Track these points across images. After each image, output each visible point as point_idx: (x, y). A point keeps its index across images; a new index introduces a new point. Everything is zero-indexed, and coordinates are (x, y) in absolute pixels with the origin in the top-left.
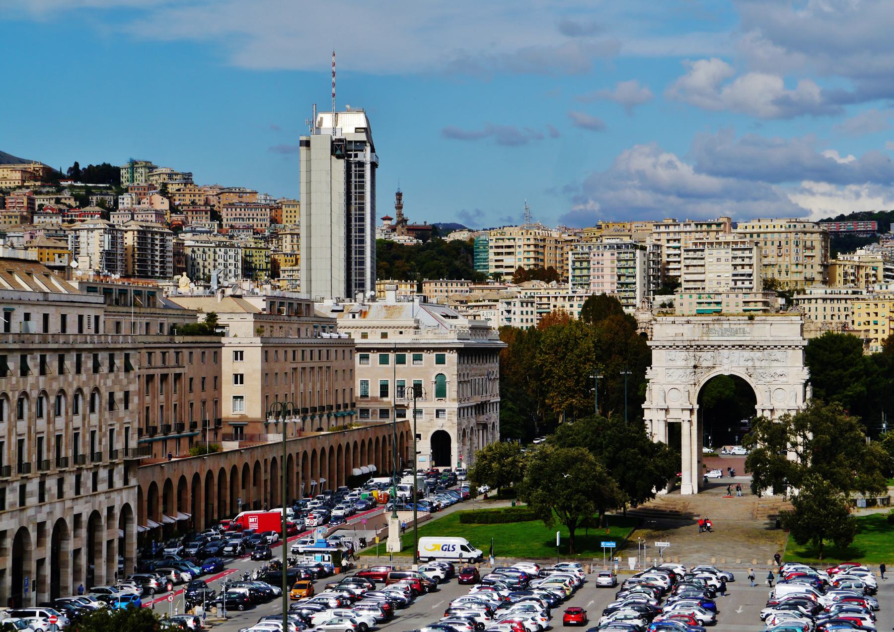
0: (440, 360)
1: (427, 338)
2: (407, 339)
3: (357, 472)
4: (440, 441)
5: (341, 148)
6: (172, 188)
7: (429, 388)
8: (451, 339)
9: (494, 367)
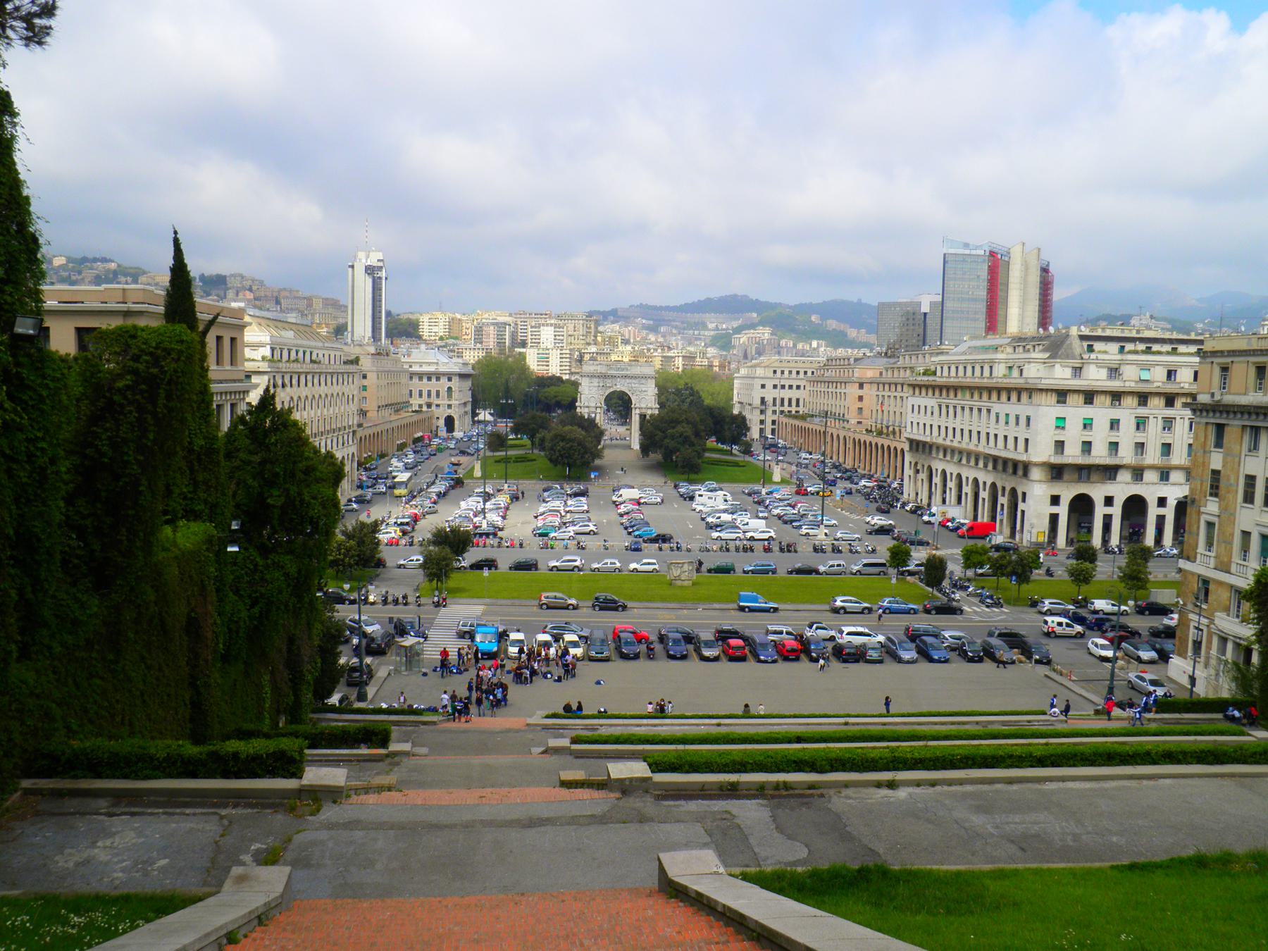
0: (450, 380)
1: (442, 369)
2: (432, 369)
3: (416, 436)
4: (450, 422)
5: (370, 270)
6: (254, 288)
7: (444, 393)
8: (456, 369)
9: (469, 383)
